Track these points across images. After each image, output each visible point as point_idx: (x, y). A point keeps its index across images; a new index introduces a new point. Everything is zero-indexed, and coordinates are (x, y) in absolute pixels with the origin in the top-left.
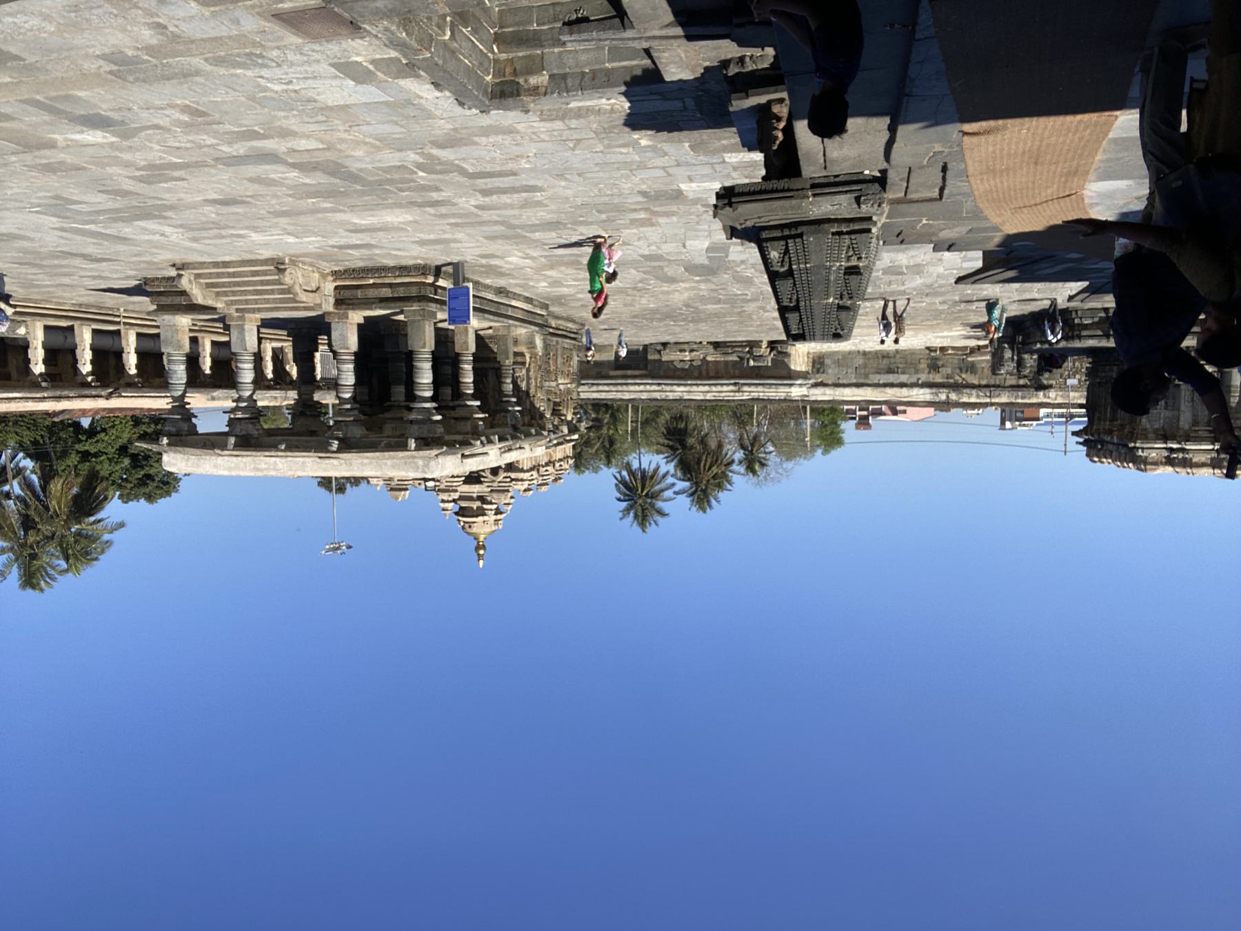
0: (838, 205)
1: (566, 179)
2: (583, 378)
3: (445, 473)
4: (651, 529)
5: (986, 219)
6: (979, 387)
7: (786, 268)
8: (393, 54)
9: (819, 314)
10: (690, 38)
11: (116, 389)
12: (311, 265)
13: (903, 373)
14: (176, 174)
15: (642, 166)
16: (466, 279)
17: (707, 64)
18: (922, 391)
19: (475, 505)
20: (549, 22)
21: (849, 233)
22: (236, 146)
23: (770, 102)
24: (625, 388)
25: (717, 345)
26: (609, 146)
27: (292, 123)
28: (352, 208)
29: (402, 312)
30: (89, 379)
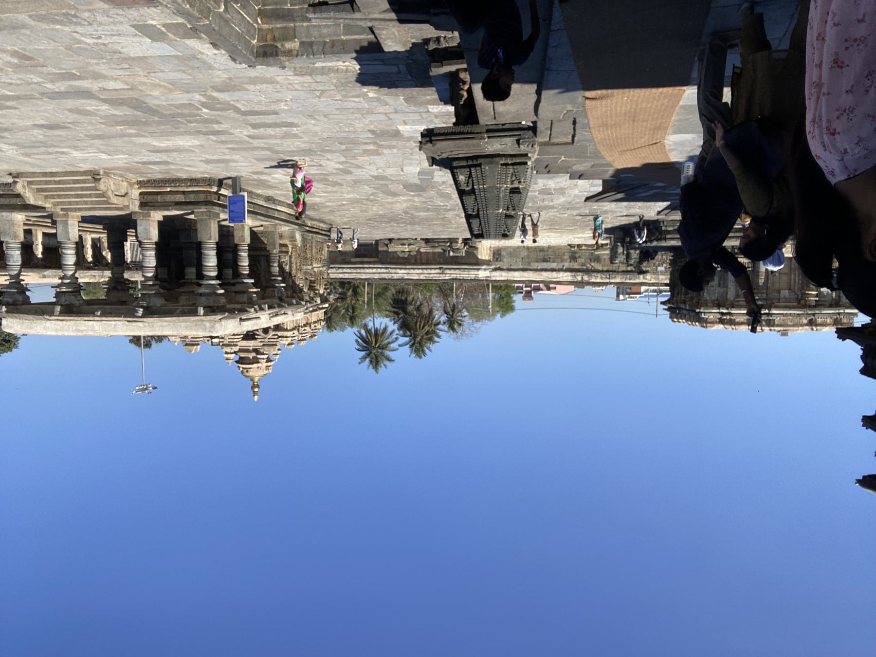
0: (504, 145)
1: (315, 119)
2: (332, 263)
3: (227, 332)
4: (382, 369)
5: (603, 158)
6: (602, 272)
7: (470, 188)
8: (181, 20)
9: (492, 221)
10: (401, 21)
12: (121, 176)
13: (554, 262)
14: (9, 104)
15: (370, 112)
16: (241, 190)
17: (414, 41)
19: (251, 355)
20: (299, 4)
21: (513, 164)
22: (58, 84)
23: (458, 71)
24: (362, 270)
25: (427, 241)
26: (345, 96)
27: (103, 69)
28: (152, 134)
29: (192, 213)
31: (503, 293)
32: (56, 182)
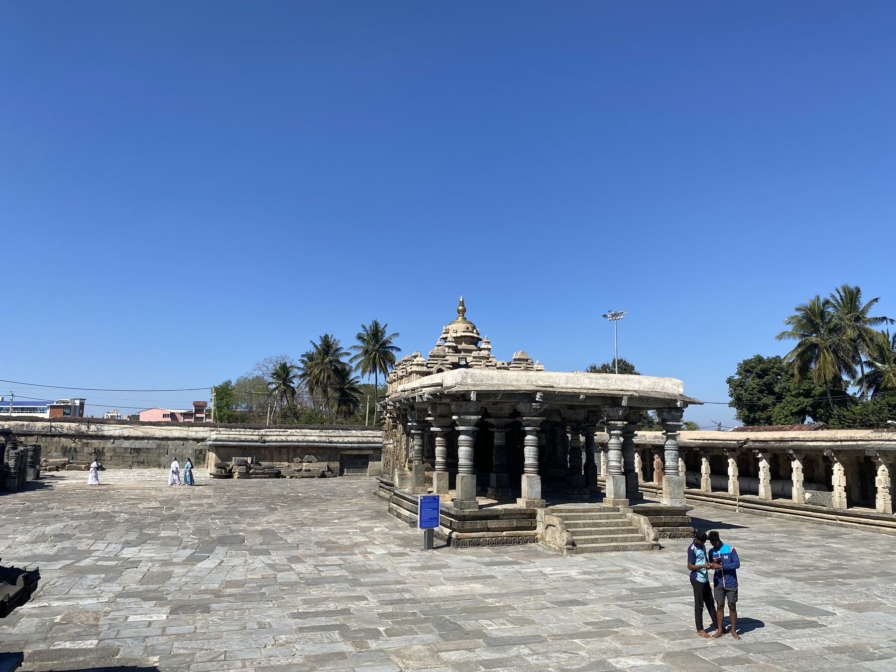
4: (368, 324)
11: (741, 447)
12: (550, 548)
14: (589, 628)
18: (111, 433)
19: (463, 346)
22: (515, 653)
24: (361, 439)
25: (278, 475)
28: (472, 597)
29: (481, 507)
30: (760, 455)
31: (225, 411)
32: (616, 540)
